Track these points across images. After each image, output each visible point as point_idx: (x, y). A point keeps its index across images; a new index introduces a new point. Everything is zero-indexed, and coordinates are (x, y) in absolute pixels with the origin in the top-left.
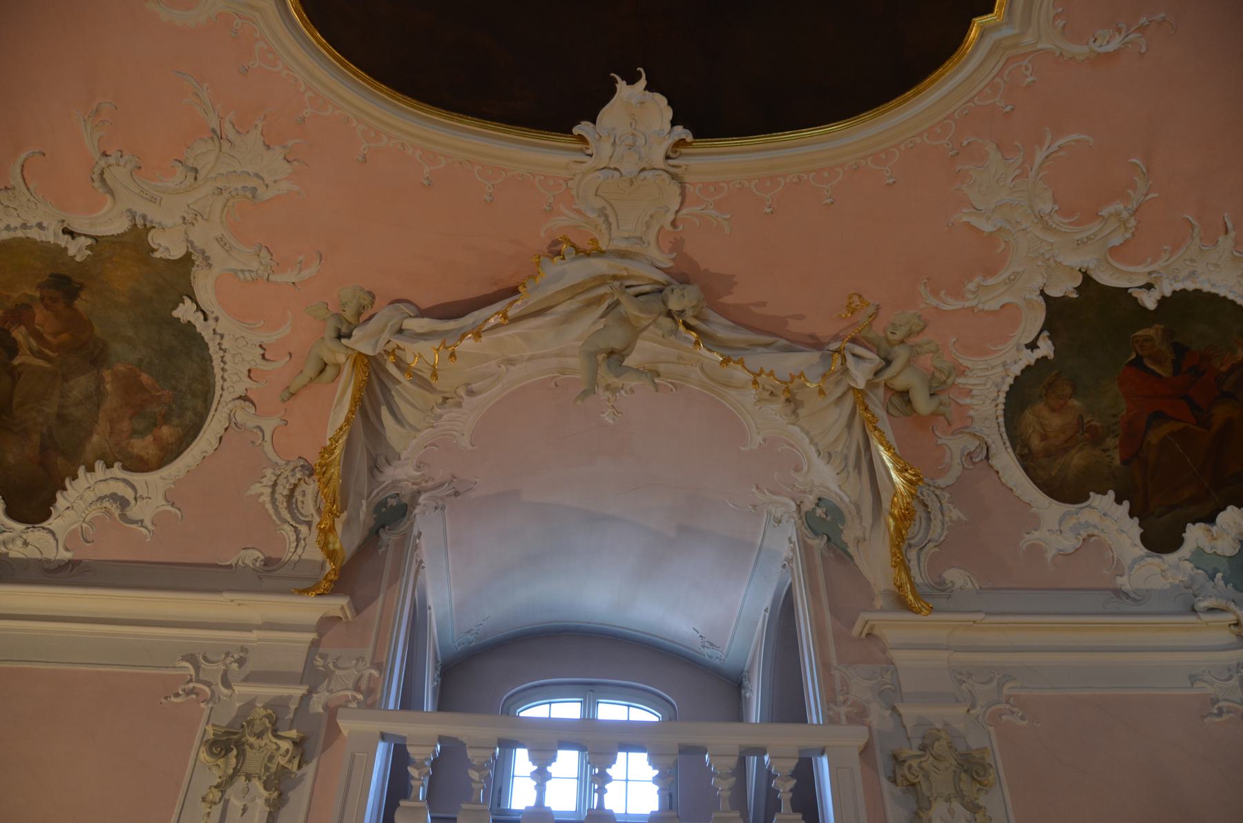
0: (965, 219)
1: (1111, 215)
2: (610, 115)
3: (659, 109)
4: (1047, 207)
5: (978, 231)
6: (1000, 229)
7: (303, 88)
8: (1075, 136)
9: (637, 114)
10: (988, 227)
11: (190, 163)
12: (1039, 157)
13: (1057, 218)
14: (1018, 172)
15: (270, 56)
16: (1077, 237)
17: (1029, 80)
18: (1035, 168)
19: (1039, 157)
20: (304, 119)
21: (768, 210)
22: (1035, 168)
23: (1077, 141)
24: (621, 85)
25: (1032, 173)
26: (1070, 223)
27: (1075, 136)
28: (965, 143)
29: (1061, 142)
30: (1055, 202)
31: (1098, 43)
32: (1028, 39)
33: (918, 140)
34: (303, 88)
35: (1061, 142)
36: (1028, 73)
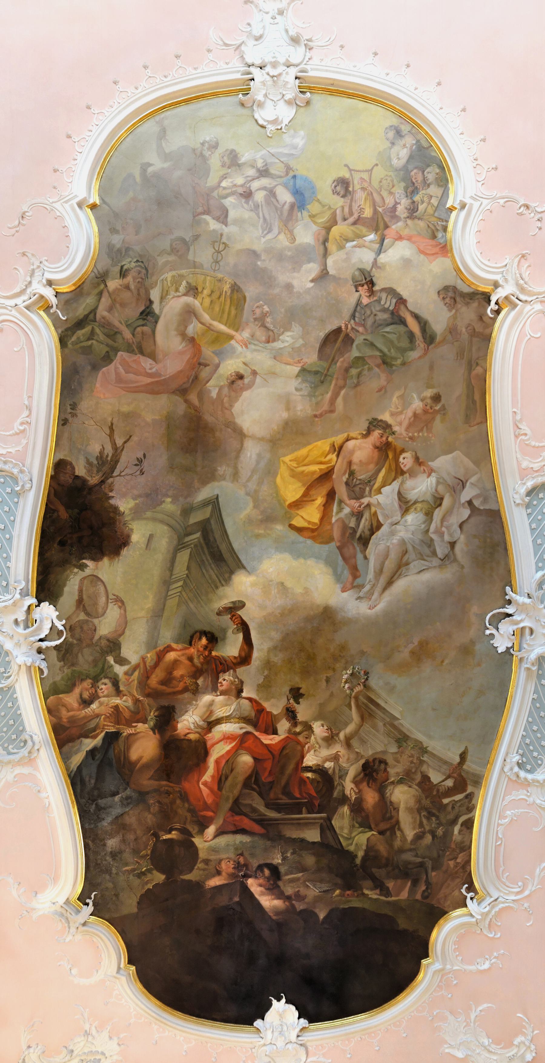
0: (447, 1051)
1: (519, 1043)
2: (269, 1015)
3: (292, 1011)
4: (486, 1041)
5: (454, 1057)
6: (467, 1055)
7: (132, 1010)
8: (485, 1005)
9: (282, 1013)
10: (460, 1055)
11: (71, 1048)
12: (473, 1016)
13: (493, 1046)
14: (465, 1024)
15: (120, 997)
16: (508, 1055)
17: (455, 982)
18: (472, 1021)
19: (473, 1016)
20: (130, 1024)
21: (349, 1056)
22: (472, 1021)
23: (488, 1007)
24: (274, 1002)
25: (472, 1024)
26: (501, 1048)
27: (485, 1005)
28: (435, 1013)
29: (480, 1008)
30: (489, 1038)
31: (479, 964)
32: (448, 967)
33: (413, 1014)
34: (132, 1010)
35: (480, 1008)
36: (453, 979)
